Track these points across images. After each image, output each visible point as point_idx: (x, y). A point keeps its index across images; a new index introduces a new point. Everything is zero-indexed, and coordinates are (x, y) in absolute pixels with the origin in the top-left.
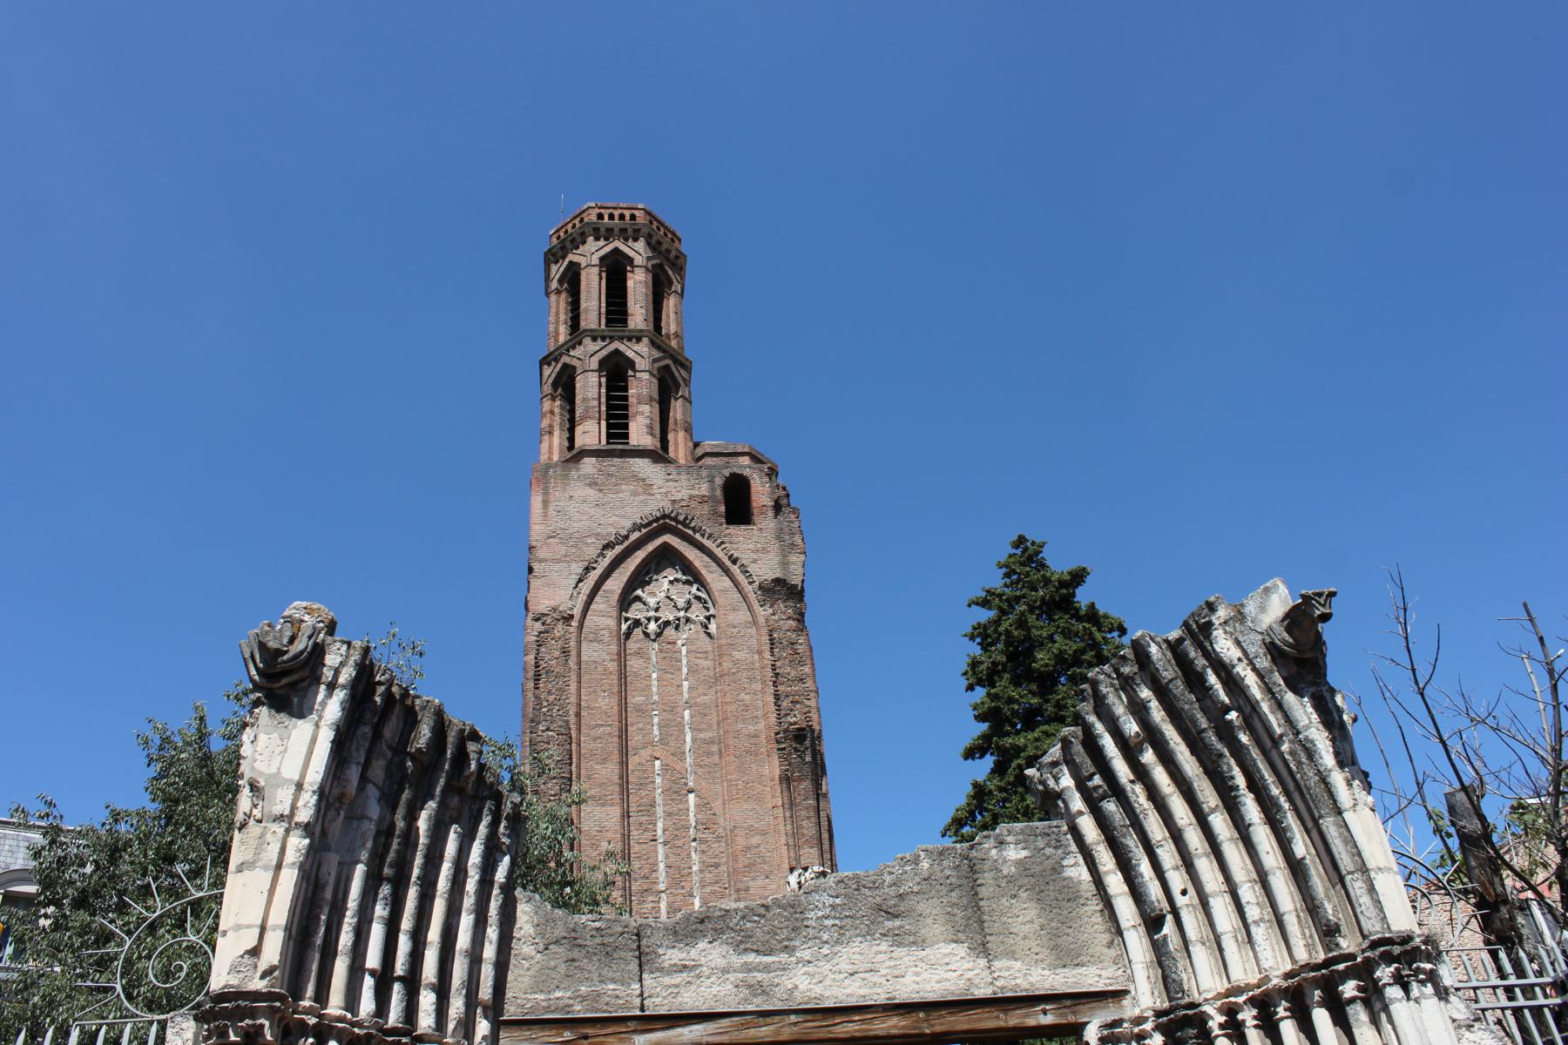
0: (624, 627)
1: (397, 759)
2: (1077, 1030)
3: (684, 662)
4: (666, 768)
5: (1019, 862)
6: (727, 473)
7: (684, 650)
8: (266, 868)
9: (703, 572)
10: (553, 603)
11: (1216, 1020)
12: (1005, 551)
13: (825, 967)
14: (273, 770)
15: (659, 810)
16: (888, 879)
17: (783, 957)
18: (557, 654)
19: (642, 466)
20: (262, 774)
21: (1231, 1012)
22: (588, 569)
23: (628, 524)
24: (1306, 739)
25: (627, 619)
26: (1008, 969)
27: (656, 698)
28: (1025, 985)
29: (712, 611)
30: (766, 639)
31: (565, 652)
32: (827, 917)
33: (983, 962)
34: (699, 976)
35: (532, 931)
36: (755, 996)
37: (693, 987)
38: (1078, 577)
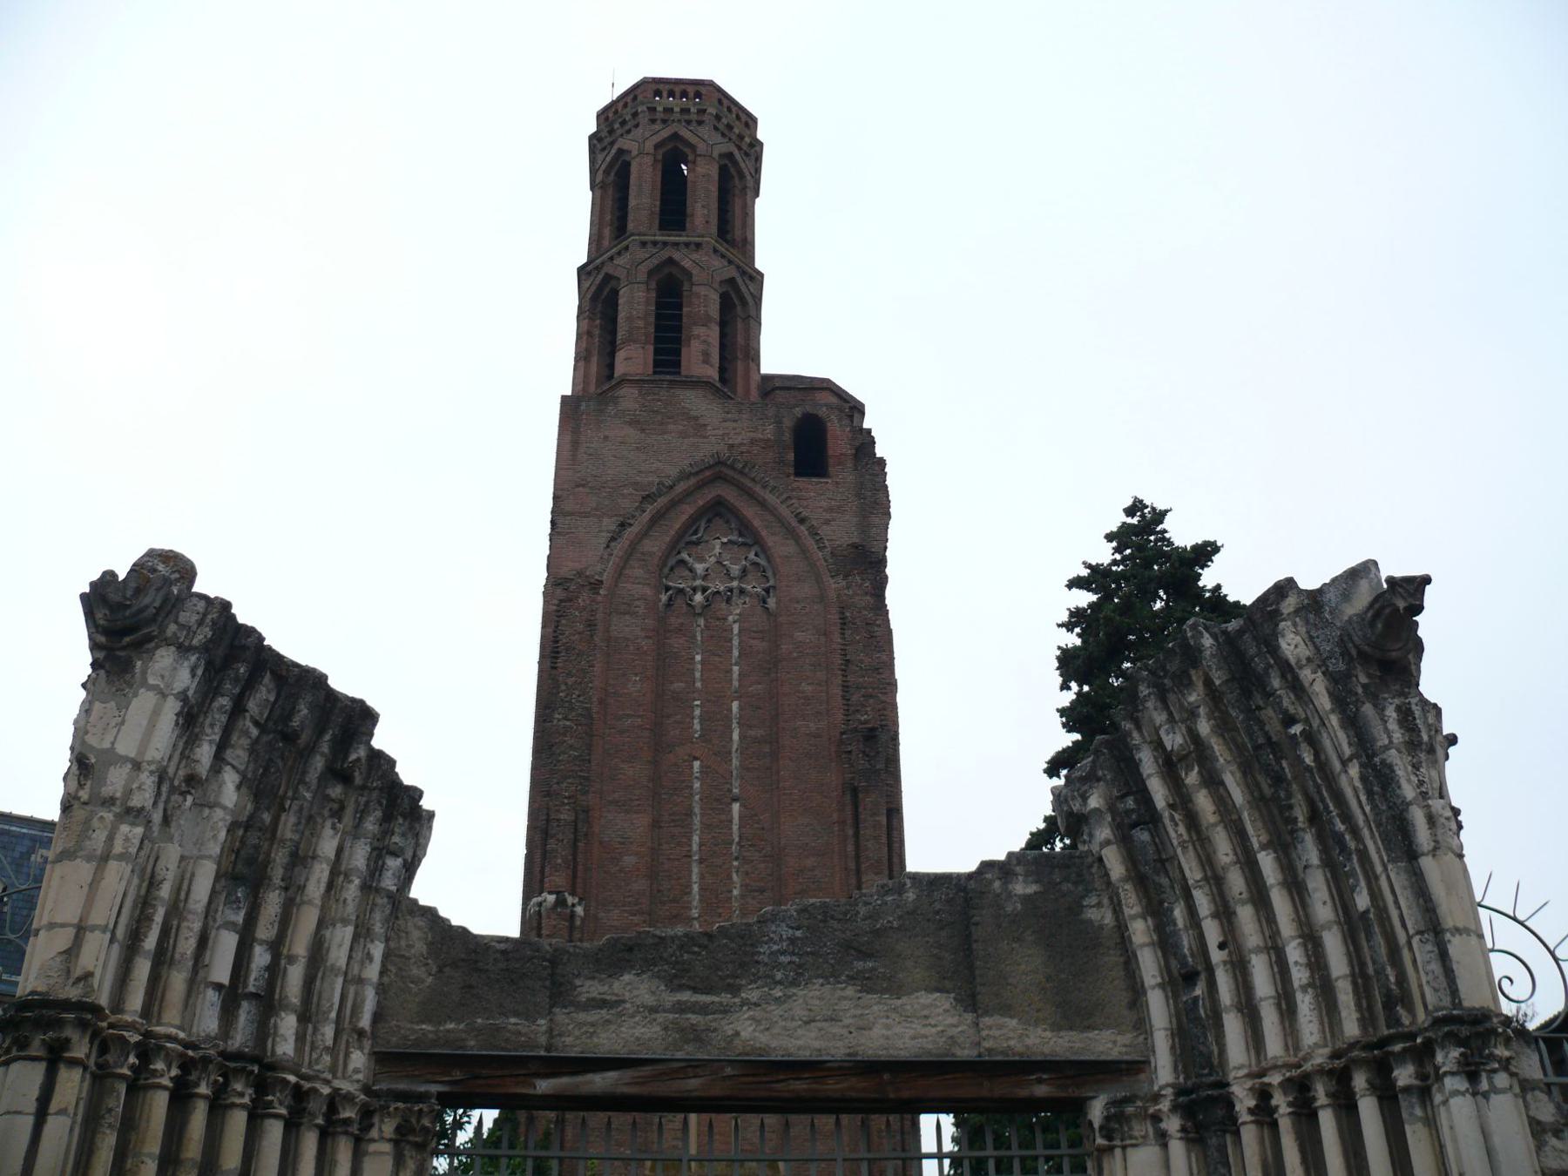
0: (664, 598)
3: (736, 642)
4: (705, 770)
5: (1026, 899)
6: (798, 412)
7: (736, 628)
8: (89, 859)
9: (764, 533)
11: (1244, 1101)
12: (1116, 519)
13: (776, 1011)
14: (106, 745)
15: (697, 820)
16: (863, 910)
17: (725, 998)
18: (580, 627)
20: (92, 748)
21: (1264, 1095)
22: (623, 525)
23: (673, 472)
24: (1383, 762)
25: (668, 589)
26: (1000, 1027)
27: (698, 684)
28: (1019, 1048)
29: (771, 583)
30: (834, 617)
31: (591, 625)
32: (783, 953)
33: (969, 1017)
34: (620, 1015)
35: (424, 950)
36: (687, 1042)
37: (613, 1027)
38: (1205, 552)
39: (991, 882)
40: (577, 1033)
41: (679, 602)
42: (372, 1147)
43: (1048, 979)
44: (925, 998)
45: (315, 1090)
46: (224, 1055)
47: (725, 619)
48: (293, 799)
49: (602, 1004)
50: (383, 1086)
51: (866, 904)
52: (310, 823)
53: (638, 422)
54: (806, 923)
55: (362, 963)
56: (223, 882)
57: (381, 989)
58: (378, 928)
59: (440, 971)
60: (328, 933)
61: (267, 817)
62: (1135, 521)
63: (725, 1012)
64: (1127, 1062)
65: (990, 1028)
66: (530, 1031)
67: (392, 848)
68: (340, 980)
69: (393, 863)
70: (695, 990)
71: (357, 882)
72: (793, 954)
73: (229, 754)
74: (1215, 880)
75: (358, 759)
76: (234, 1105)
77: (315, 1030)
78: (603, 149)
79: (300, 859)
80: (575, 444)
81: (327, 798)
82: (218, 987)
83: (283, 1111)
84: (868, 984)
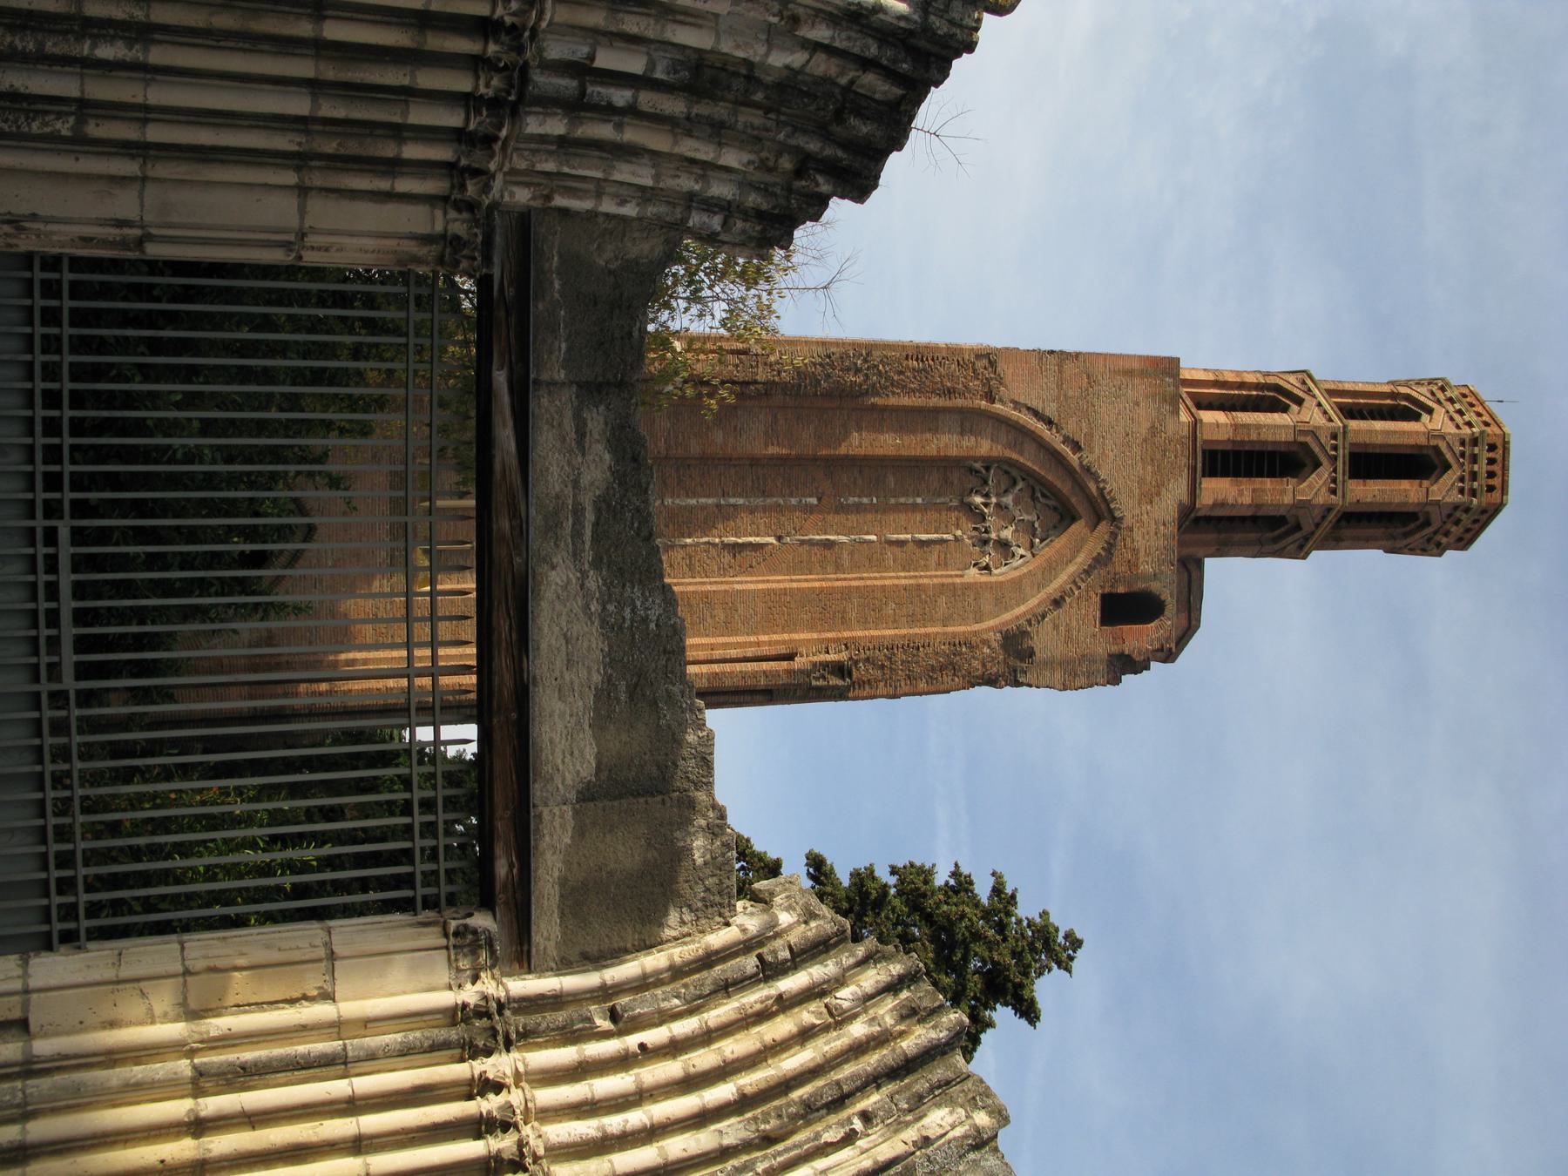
0: (978, 466)
1: (837, 91)
2: (487, 903)
10: (1008, 378)
12: (1062, 922)
16: (676, 689)
17: (589, 556)
19: (1177, 490)
22: (1049, 422)
25: (987, 469)
26: (563, 826)
28: (543, 845)
32: (633, 611)
33: (572, 796)
34: (571, 451)
35: (632, 256)
37: (558, 444)
38: (1028, 1011)
39: (705, 816)
40: (552, 409)
41: (974, 481)
42: (439, 213)
43: (611, 874)
44: (590, 753)
45: (492, 156)
46: (525, 69)
47: (958, 527)
48: (778, 122)
49: (581, 433)
50: (498, 221)
51: (682, 693)
52: (752, 140)
53: (1154, 435)
54: (663, 634)
55: (616, 196)
56: (694, 56)
57: (592, 215)
58: (651, 210)
59: (610, 272)
60: (646, 160)
61: (759, 97)
62: (1060, 939)
63: (575, 555)
64: (529, 952)
65: (562, 816)
66: (553, 363)
67: (731, 221)
68: (599, 175)
69: (716, 222)
70: (596, 524)
71: (697, 187)
72: (632, 620)
73: (821, 57)
74: (707, 1037)
75: (817, 185)
76: (477, 78)
77: (550, 153)
78: (1433, 394)
79: (718, 131)
80: (1129, 373)
81: (779, 154)
82: (592, 58)
83: (472, 127)
84: (604, 695)
